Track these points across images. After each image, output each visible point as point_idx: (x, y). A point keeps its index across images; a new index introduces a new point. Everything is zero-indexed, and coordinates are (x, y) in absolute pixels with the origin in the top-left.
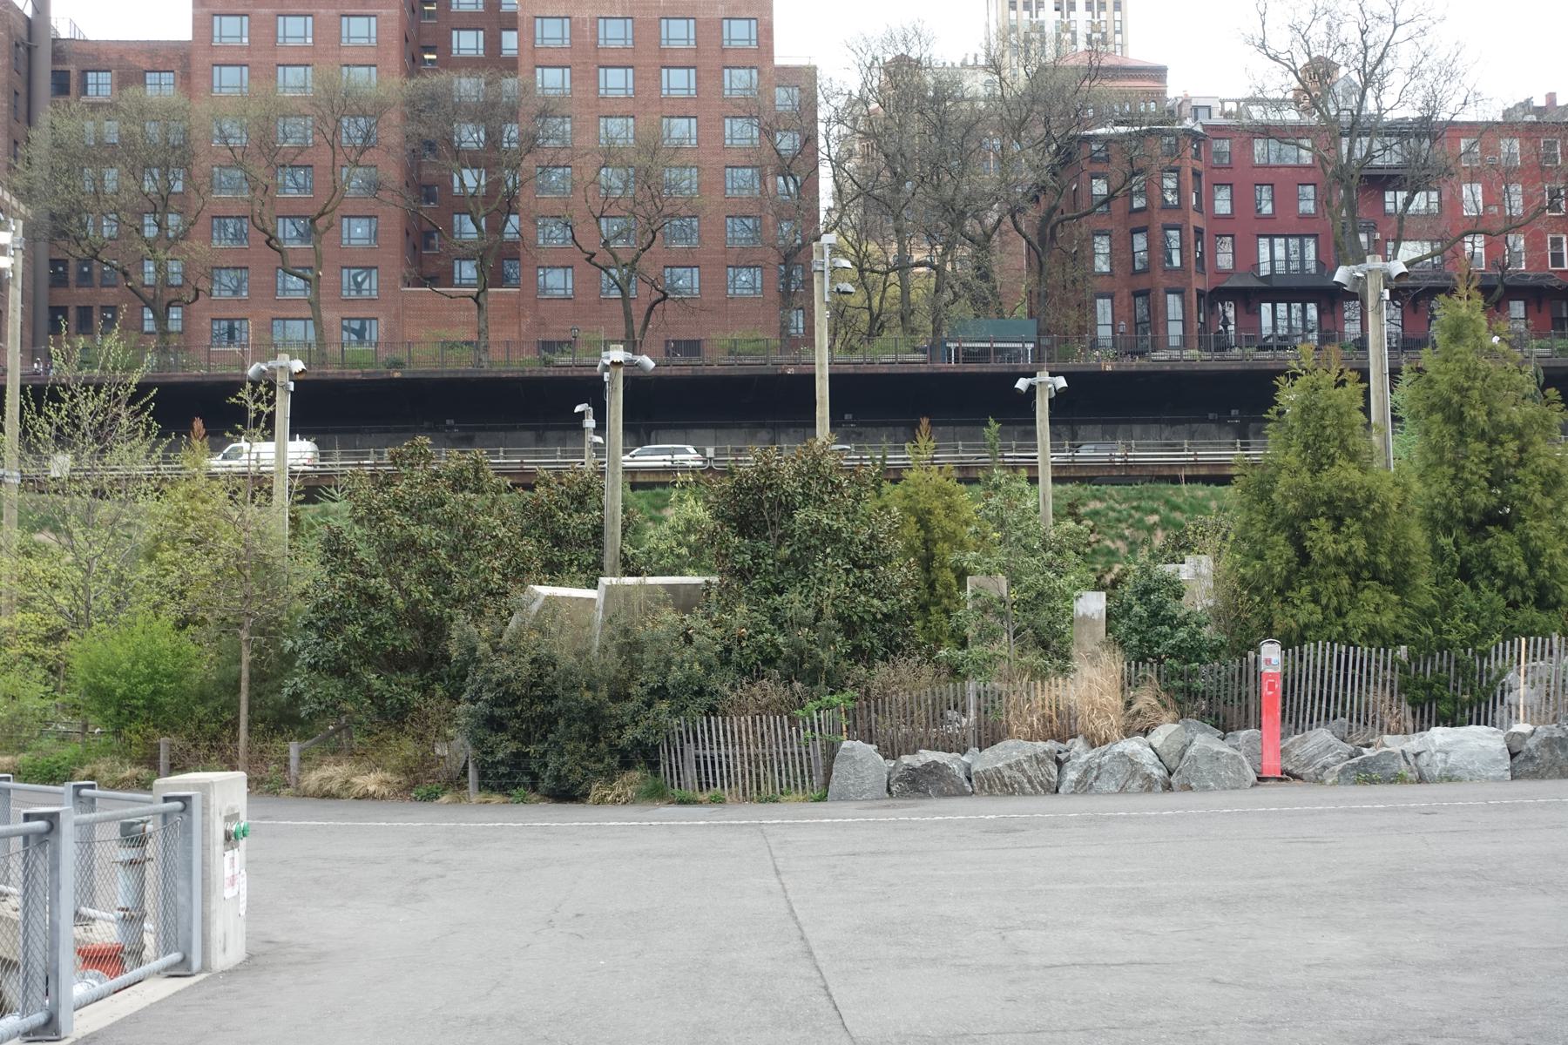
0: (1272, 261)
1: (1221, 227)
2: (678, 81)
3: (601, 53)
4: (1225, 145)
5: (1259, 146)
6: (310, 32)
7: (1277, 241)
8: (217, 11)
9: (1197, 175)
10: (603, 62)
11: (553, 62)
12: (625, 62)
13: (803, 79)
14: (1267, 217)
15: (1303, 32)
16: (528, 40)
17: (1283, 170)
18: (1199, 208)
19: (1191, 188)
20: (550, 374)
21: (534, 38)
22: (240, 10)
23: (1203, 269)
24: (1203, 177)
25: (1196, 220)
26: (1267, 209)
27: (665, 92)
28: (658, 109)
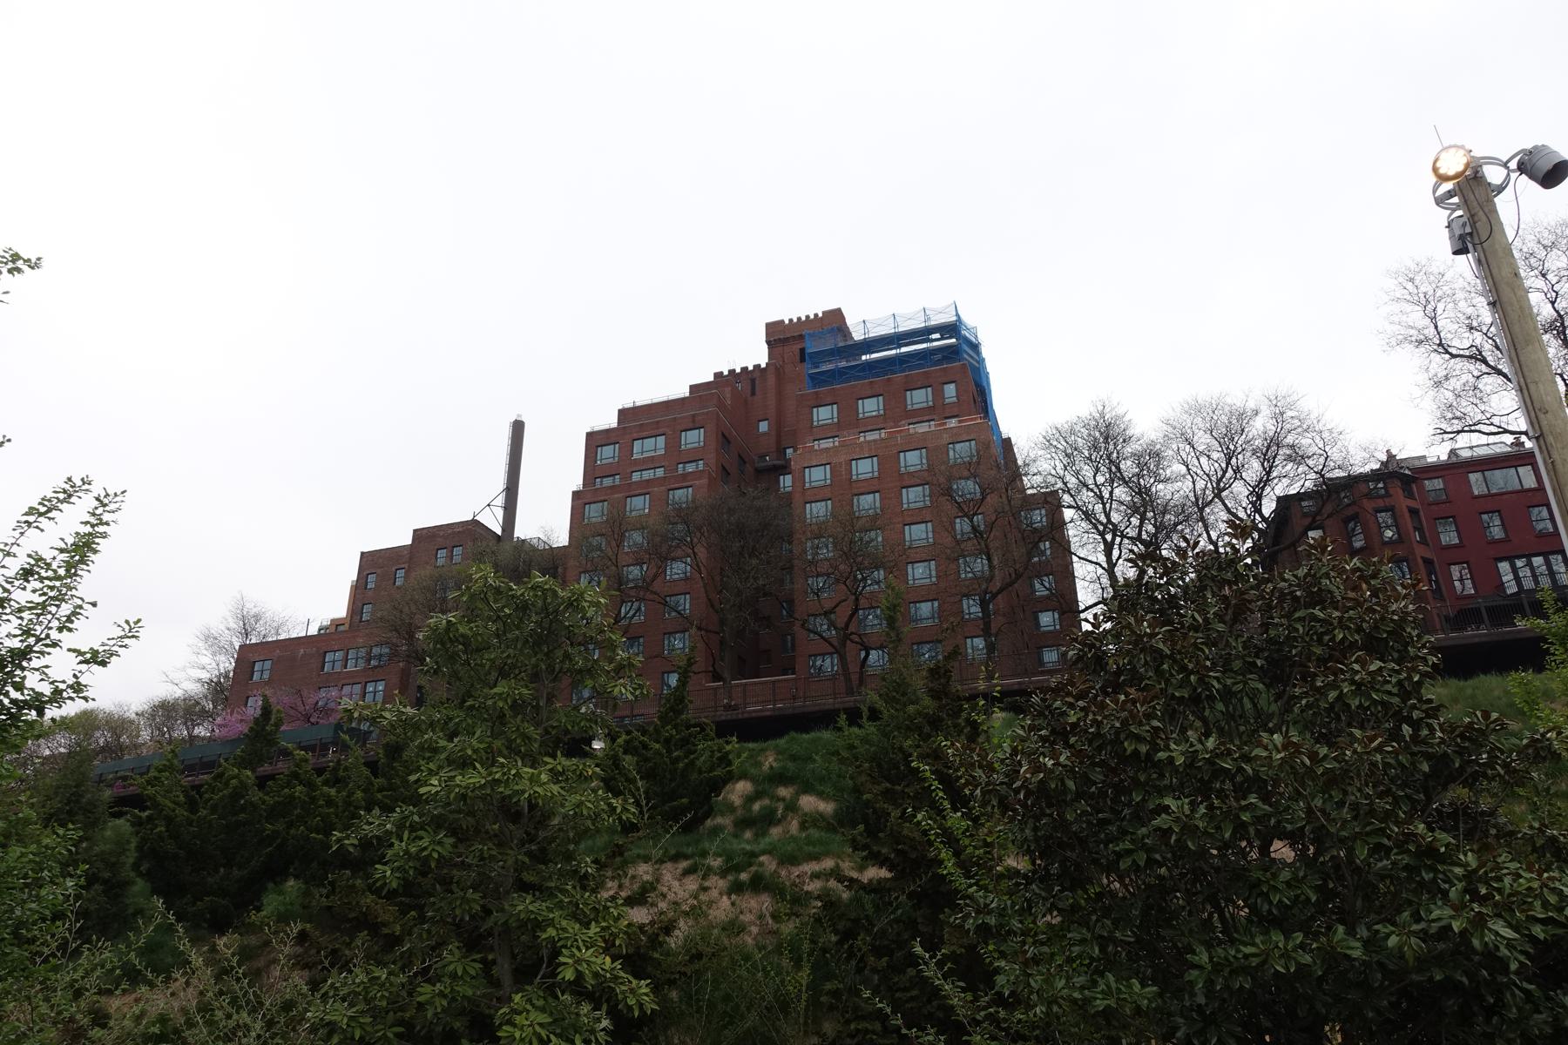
0: (1517, 578)
1: (1454, 555)
2: (914, 496)
3: (854, 485)
4: (1438, 484)
5: (1474, 478)
6: (647, 506)
7: (1519, 563)
8: (586, 501)
9: (1414, 512)
10: (856, 491)
11: (818, 498)
12: (873, 488)
13: (1050, 501)
14: (1500, 541)
15: (1485, 330)
16: (800, 480)
17: (1506, 497)
18: (1424, 542)
19: (1411, 530)
20: (729, 717)
21: (804, 482)
22: (602, 498)
23: (1442, 596)
24: (1422, 513)
25: (1421, 552)
26: (1497, 532)
27: (905, 506)
28: (900, 519)
